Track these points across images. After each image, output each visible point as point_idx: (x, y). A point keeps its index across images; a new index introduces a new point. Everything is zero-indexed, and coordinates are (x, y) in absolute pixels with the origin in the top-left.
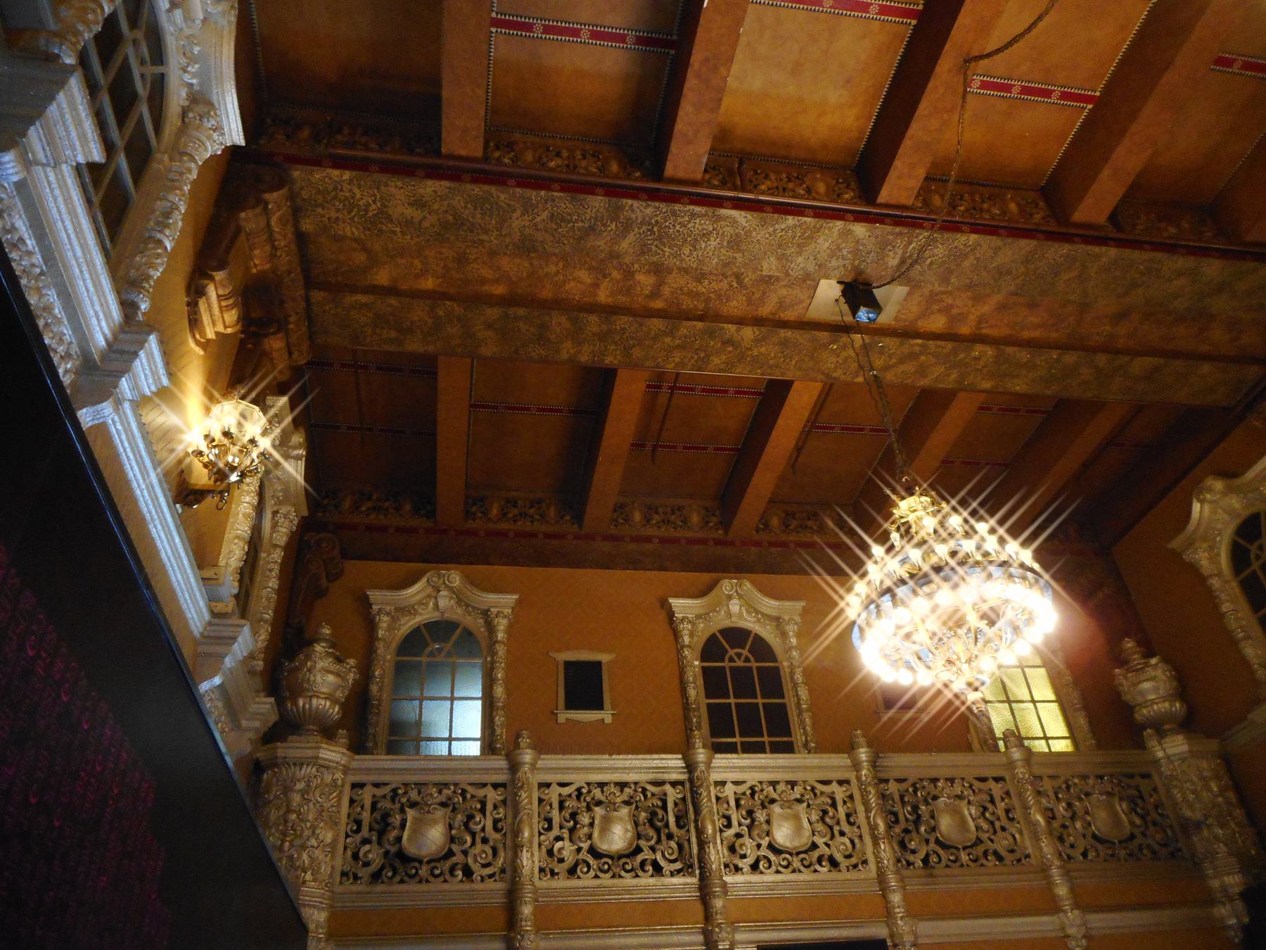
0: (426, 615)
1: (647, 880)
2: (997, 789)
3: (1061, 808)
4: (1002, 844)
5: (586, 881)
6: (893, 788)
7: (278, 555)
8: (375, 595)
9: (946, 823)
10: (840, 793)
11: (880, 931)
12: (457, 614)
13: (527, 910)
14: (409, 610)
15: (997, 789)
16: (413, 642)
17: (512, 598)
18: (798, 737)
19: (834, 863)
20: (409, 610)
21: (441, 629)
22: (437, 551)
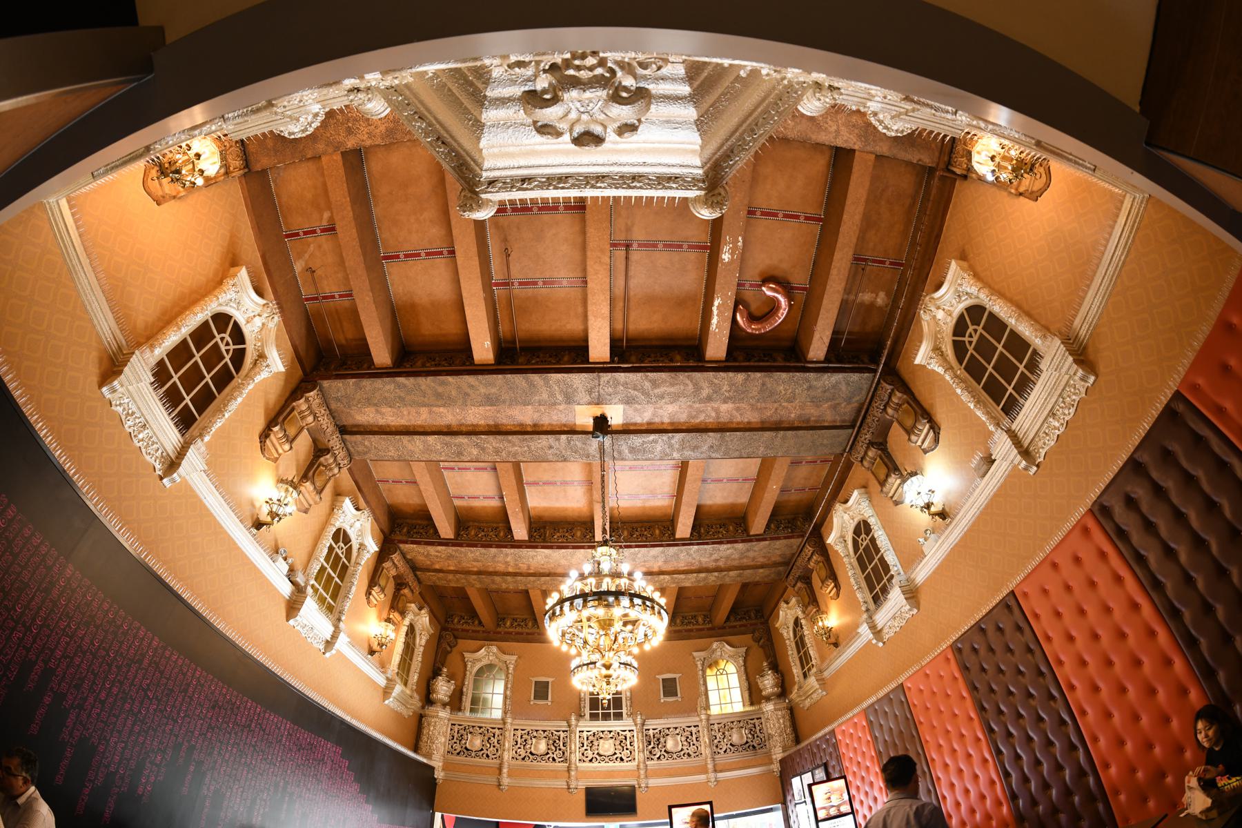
0: (485, 662)
1: (551, 764)
2: (694, 730)
3: (719, 735)
4: (691, 750)
5: (528, 762)
6: (651, 732)
7: (422, 649)
8: (466, 655)
9: (670, 745)
10: (629, 735)
11: (634, 783)
12: (496, 661)
13: (505, 770)
14: (480, 660)
15: (694, 730)
16: (480, 672)
17: (515, 657)
18: (624, 711)
19: (622, 759)
20: (480, 660)
21: (490, 667)
22: (490, 637)
